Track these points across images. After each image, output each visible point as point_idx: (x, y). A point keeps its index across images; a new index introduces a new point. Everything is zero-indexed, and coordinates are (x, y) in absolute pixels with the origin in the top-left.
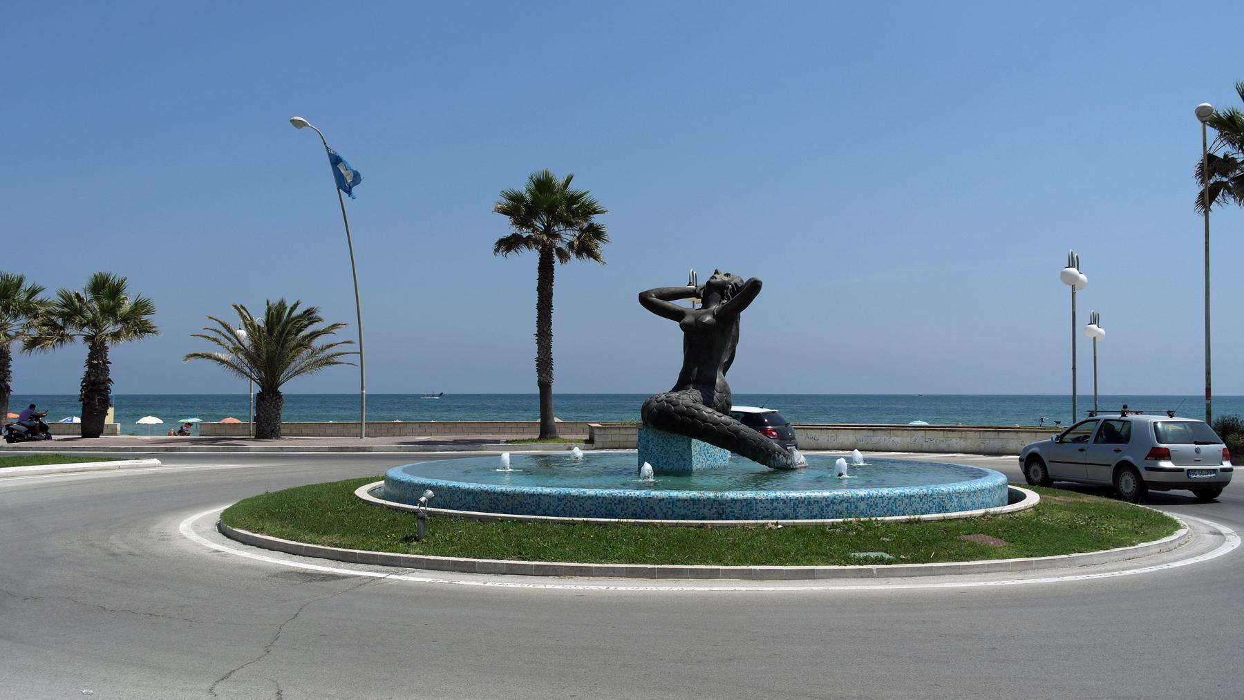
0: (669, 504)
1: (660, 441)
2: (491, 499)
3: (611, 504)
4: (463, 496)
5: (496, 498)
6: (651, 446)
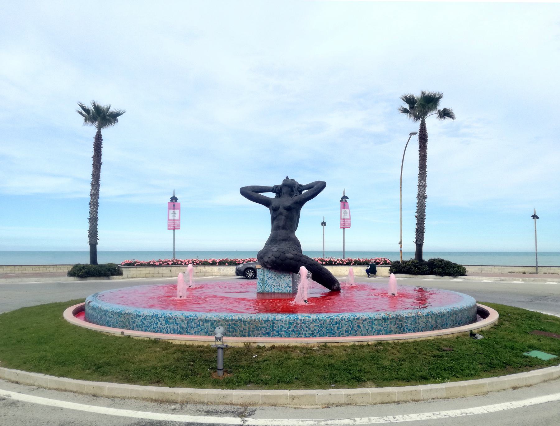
0: (370, 323)
1: (273, 276)
2: (229, 325)
3: (330, 324)
4: (201, 323)
5: (233, 324)
6: (266, 278)
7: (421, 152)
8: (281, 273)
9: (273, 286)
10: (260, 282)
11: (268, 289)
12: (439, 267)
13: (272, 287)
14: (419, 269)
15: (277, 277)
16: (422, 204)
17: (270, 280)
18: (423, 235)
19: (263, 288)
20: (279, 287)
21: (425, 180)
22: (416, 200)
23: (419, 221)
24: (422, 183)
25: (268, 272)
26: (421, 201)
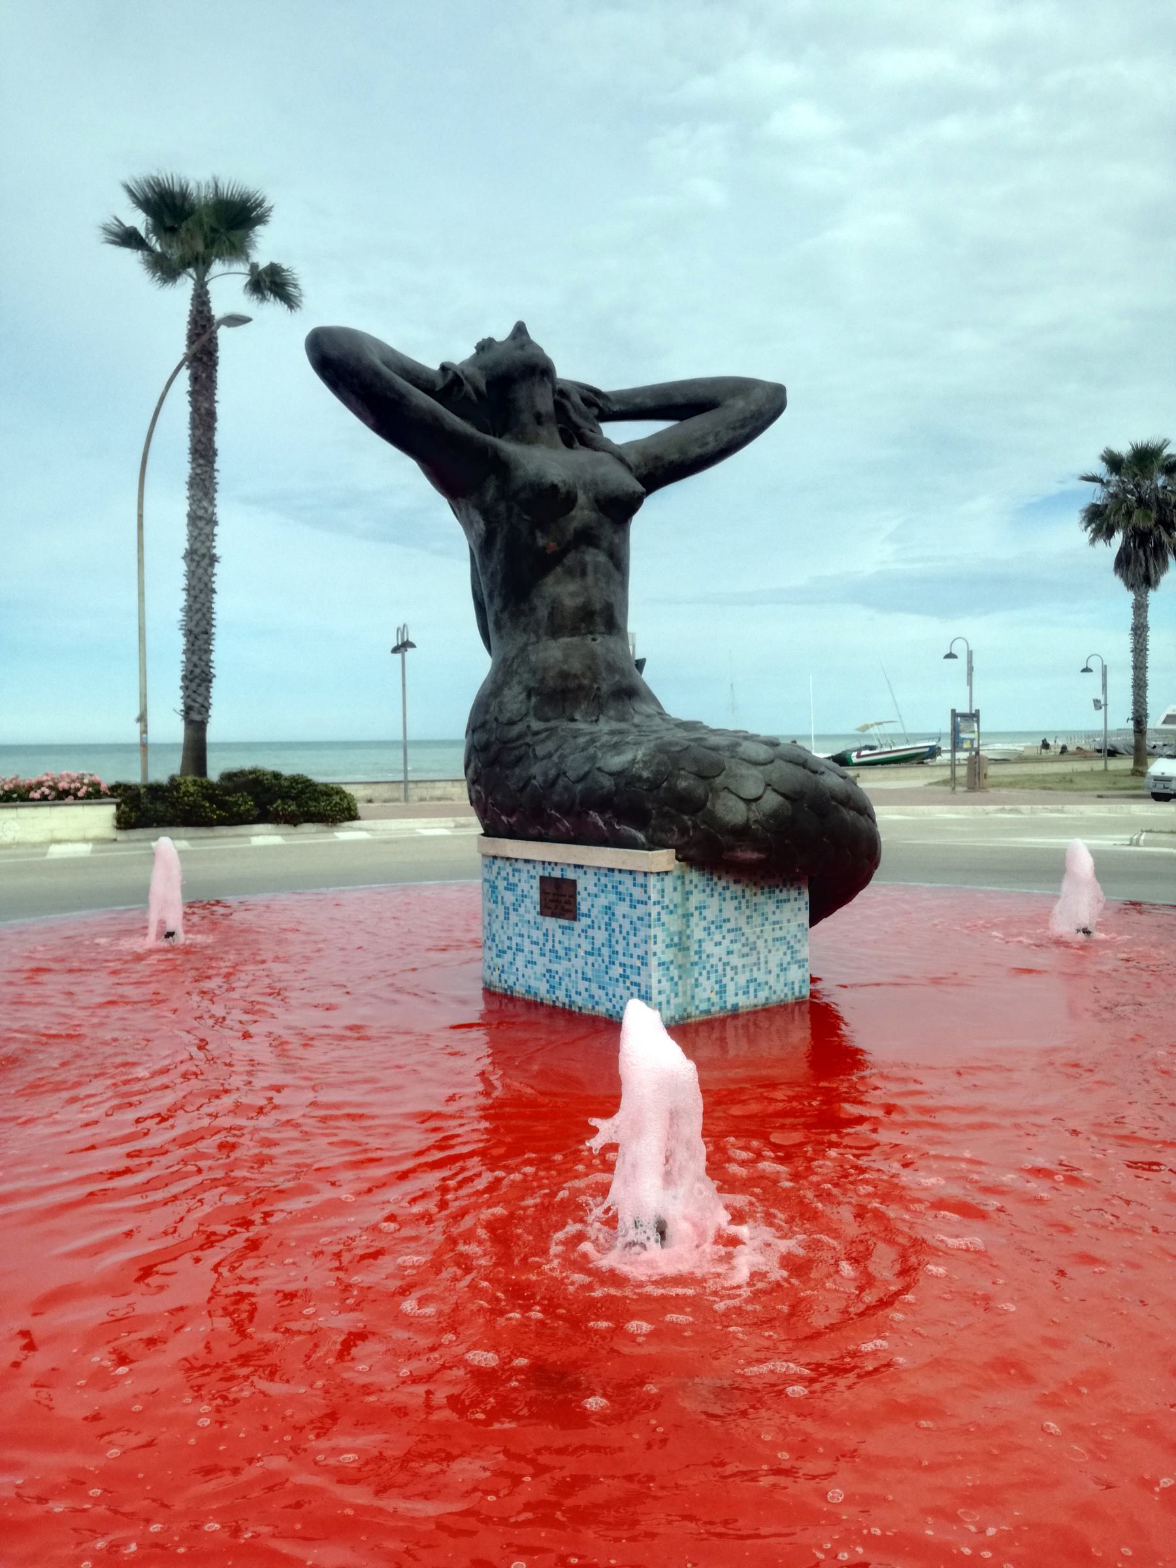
1: (729, 907)
6: (698, 933)
7: (201, 398)
8: (762, 888)
9: (728, 968)
10: (668, 956)
11: (705, 995)
12: (285, 796)
13: (725, 981)
14: (222, 805)
15: (748, 912)
16: (206, 584)
17: (717, 937)
18: (208, 689)
19: (685, 993)
20: (756, 974)
21: (212, 501)
22: (182, 567)
23: (198, 643)
24: (206, 511)
25: (704, 891)
26: (201, 571)
